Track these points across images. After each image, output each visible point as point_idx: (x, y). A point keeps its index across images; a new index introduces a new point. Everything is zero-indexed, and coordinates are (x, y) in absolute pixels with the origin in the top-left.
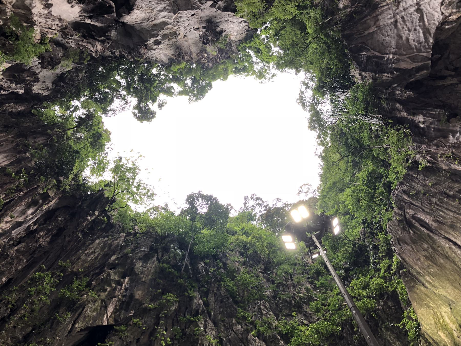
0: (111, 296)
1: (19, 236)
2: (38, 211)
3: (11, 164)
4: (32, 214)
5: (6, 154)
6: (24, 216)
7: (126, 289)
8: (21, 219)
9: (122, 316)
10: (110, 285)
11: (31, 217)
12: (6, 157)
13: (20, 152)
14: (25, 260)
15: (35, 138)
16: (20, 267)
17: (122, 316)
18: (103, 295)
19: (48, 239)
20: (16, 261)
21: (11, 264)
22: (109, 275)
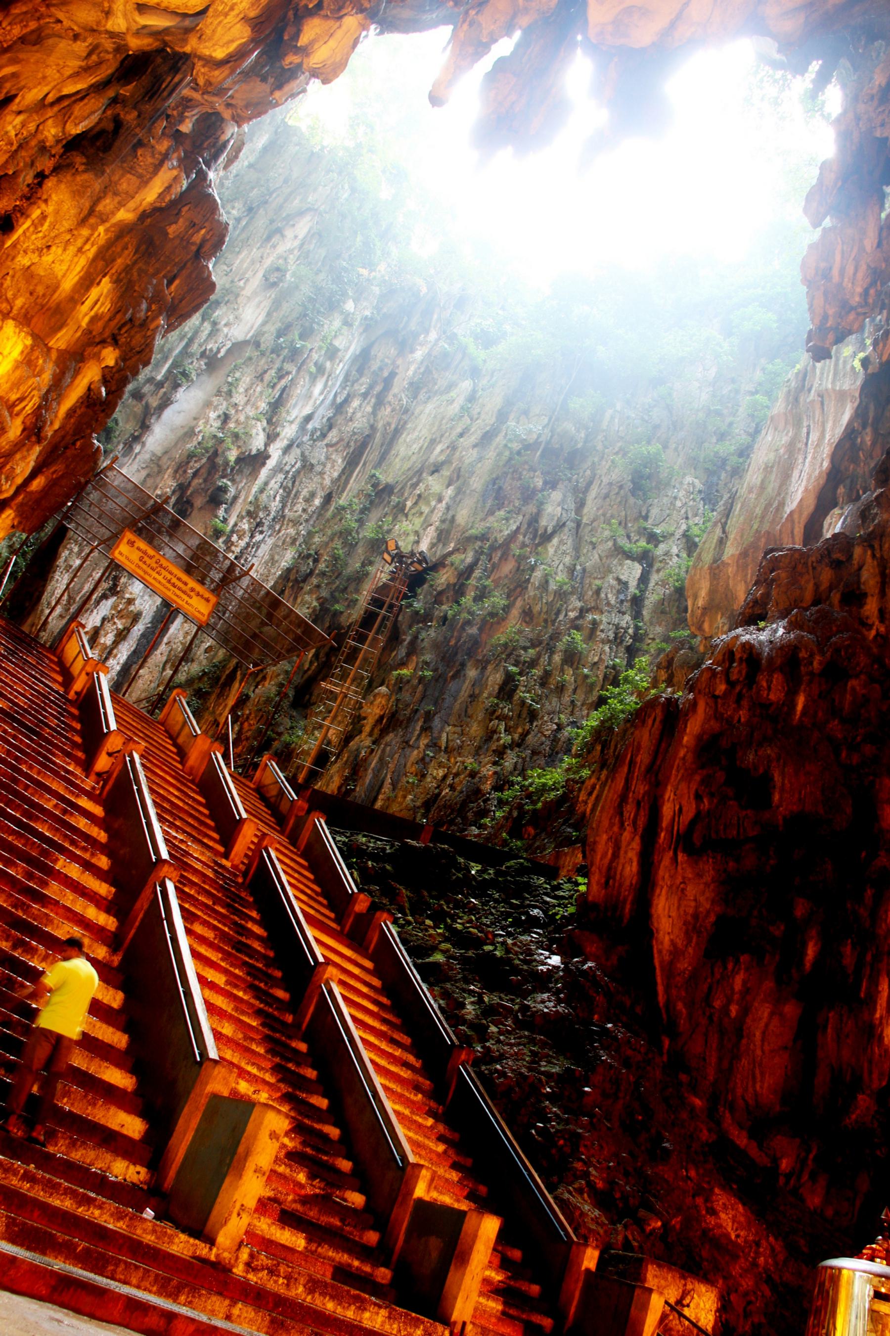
0: (427, 524)
1: (325, 420)
2: (330, 383)
3: (269, 314)
4: (321, 393)
5: (257, 300)
6: (311, 402)
7: (448, 508)
8: (307, 411)
9: (438, 553)
10: (428, 503)
11: (322, 398)
12: (258, 306)
13: (274, 284)
14: (340, 461)
15: (294, 225)
16: (336, 475)
17: (438, 553)
18: (418, 521)
19: (369, 409)
20: (329, 465)
21: (321, 474)
22: (427, 488)
